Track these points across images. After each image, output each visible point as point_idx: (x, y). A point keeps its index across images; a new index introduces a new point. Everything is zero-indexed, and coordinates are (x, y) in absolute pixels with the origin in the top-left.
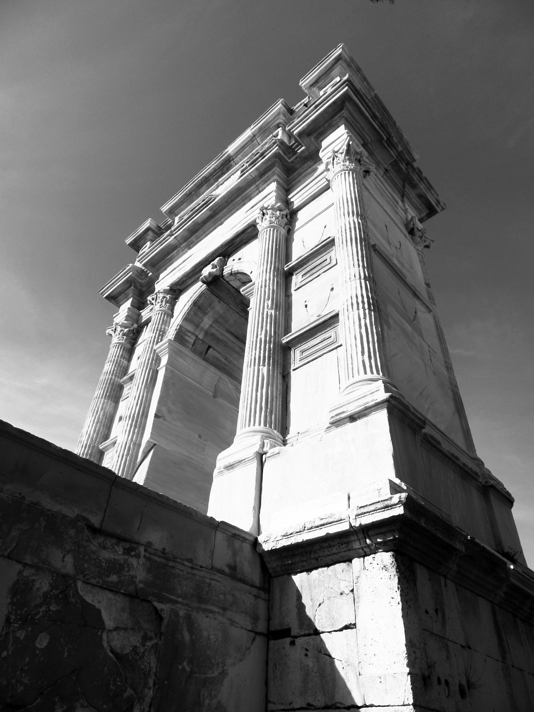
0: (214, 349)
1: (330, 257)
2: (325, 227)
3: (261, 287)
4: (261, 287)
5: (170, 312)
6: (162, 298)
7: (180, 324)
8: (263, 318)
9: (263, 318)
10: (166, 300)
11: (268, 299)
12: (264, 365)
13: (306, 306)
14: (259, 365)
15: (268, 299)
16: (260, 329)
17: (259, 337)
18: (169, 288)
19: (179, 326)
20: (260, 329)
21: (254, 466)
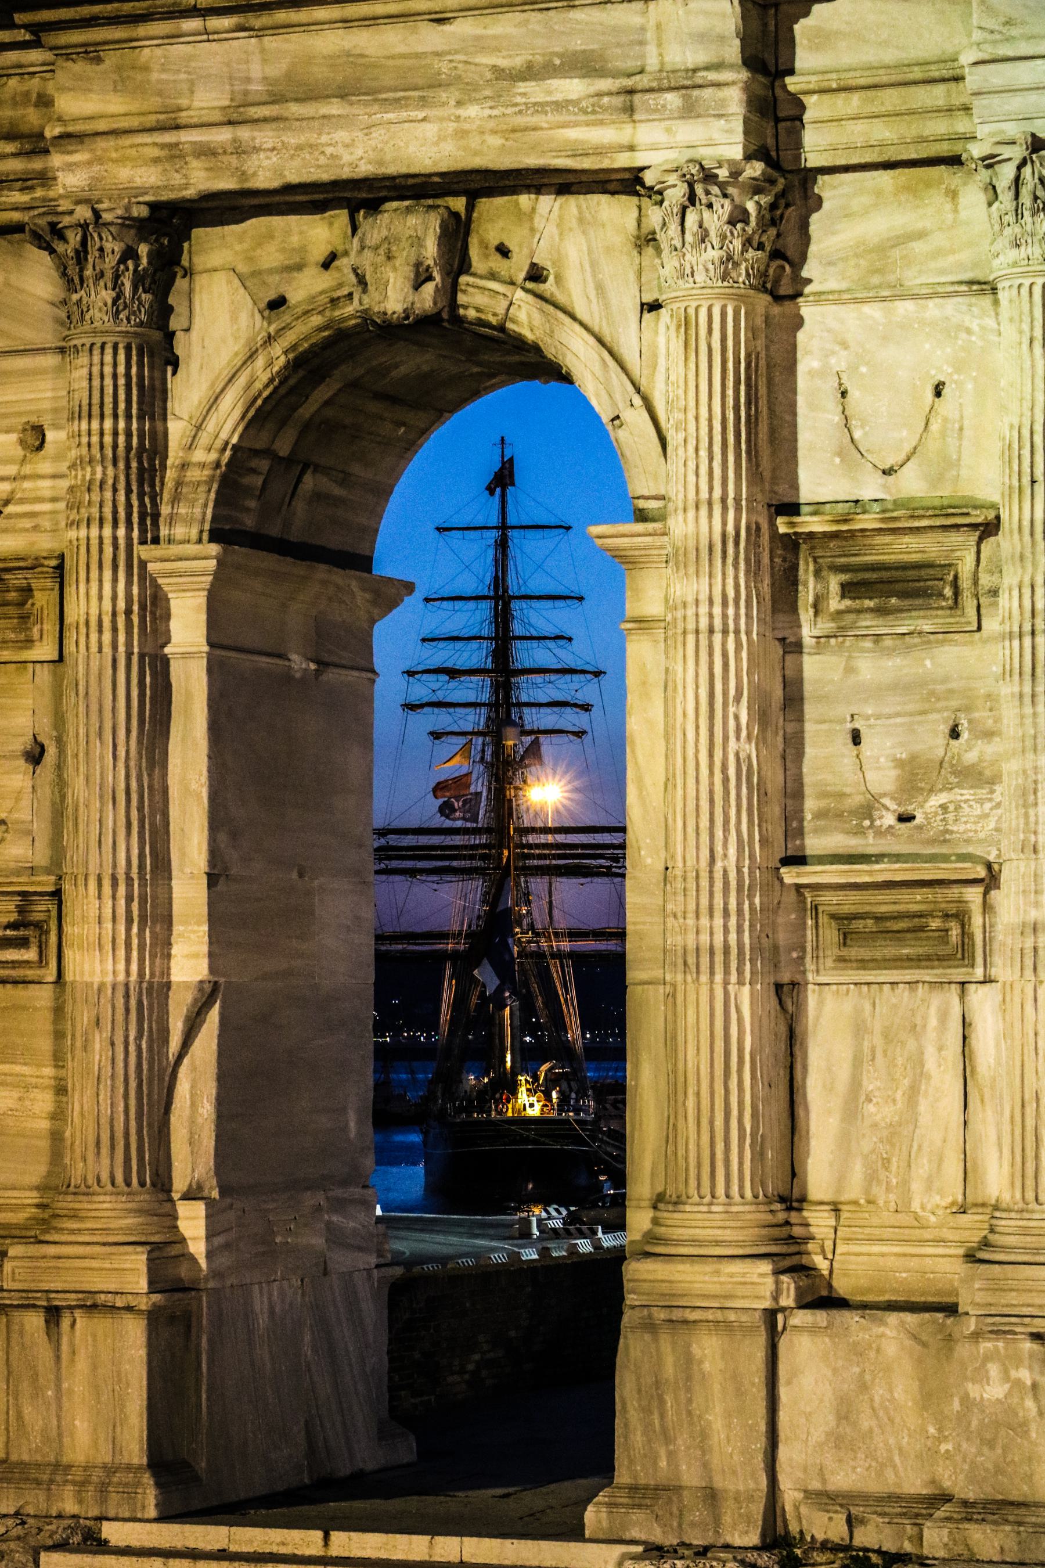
0: (317, 468)
1: (956, 577)
2: (938, 394)
3: (711, 631)
4: (711, 631)
5: (157, 335)
6: (119, 262)
7: (235, 440)
8: (726, 780)
9: (726, 780)
10: (135, 271)
11: (738, 699)
12: (741, 983)
13: (856, 738)
14: (726, 983)
15: (738, 699)
16: (719, 833)
17: (719, 865)
18: (144, 212)
19: (228, 453)
20: (719, 833)
21: (760, 1342)
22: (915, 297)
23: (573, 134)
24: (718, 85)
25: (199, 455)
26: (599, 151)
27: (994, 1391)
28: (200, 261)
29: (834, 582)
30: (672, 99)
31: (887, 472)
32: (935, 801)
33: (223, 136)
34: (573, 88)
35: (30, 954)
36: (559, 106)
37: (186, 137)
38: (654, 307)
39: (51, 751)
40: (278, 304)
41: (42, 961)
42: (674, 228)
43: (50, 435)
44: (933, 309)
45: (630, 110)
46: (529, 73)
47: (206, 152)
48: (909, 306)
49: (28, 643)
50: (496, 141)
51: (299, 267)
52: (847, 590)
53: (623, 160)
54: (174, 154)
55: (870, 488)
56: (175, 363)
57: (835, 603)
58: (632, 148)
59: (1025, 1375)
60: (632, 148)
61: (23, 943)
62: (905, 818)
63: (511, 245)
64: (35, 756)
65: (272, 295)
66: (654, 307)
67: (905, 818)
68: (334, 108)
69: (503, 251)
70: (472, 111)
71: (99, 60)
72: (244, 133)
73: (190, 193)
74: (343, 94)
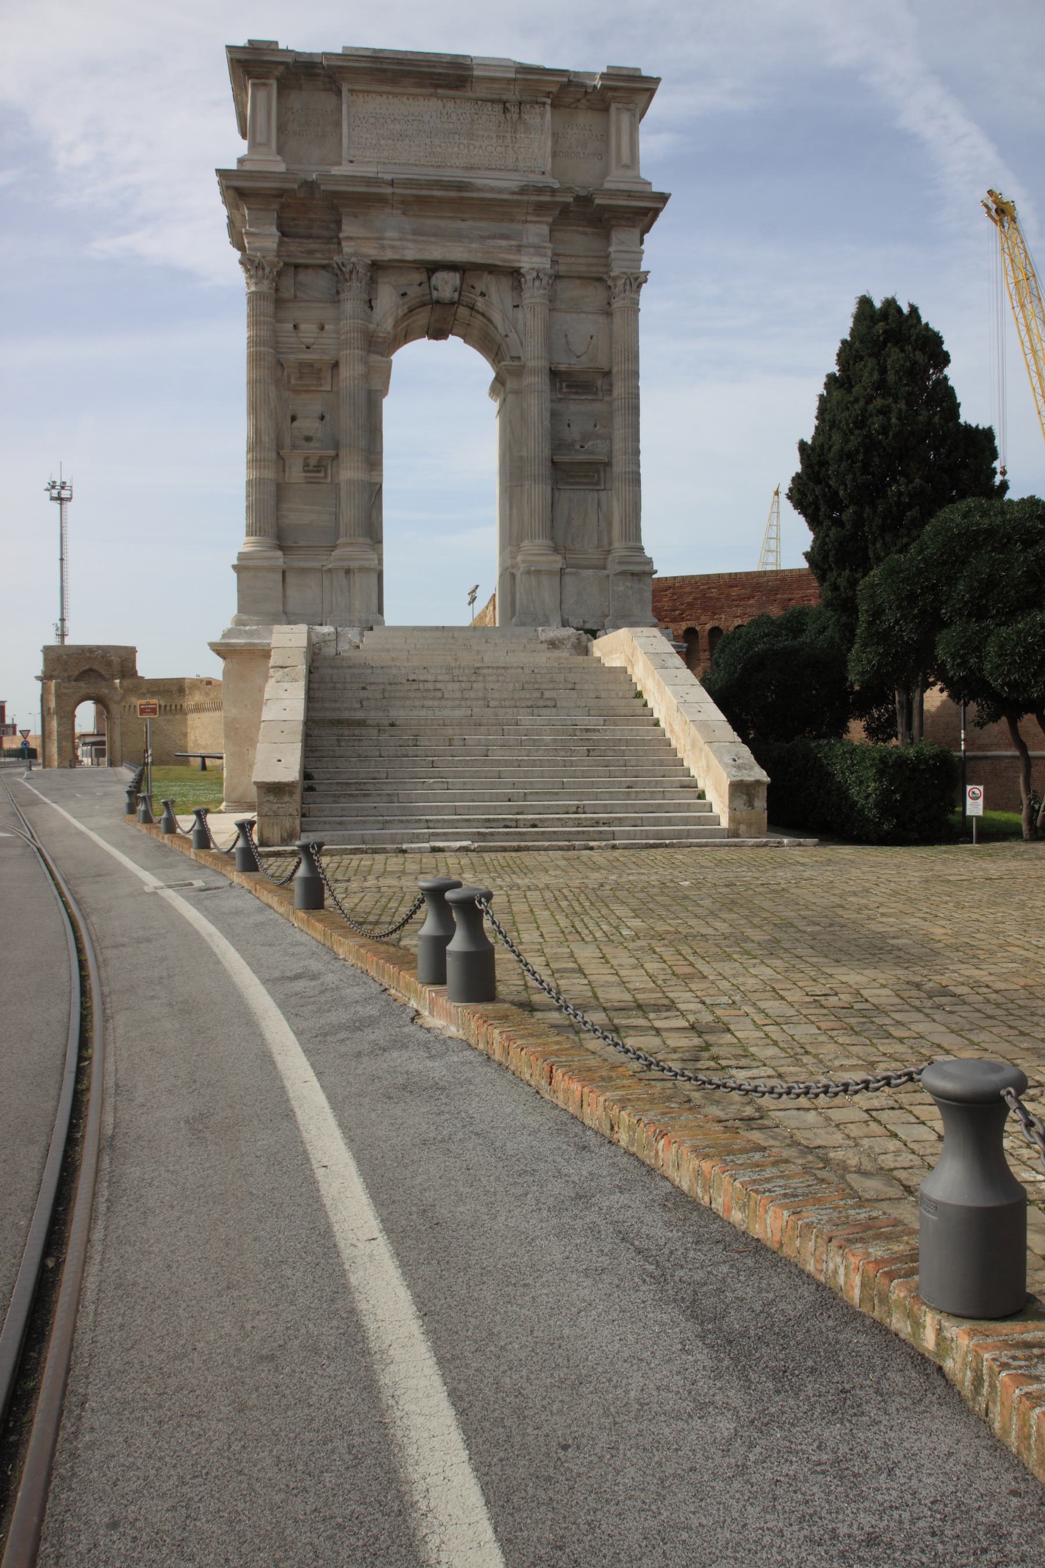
13: (569, 426)
22: (586, 313)
23: (503, 256)
24: (545, 248)
25: (381, 335)
26: (510, 261)
27: (621, 588)
28: (380, 280)
29: (564, 385)
30: (532, 250)
31: (578, 357)
32: (590, 443)
33: (398, 243)
34: (504, 243)
35: (322, 475)
36: (500, 247)
37: (386, 242)
38: (517, 306)
39: (327, 417)
40: (404, 295)
41: (326, 477)
42: (530, 284)
43: (327, 327)
44: (590, 317)
45: (519, 250)
46: (489, 237)
47: (393, 247)
48: (583, 316)
49: (321, 385)
50: (480, 255)
51: (411, 285)
52: (568, 386)
53: (517, 265)
54: (383, 247)
55: (574, 361)
56: (371, 307)
57: (565, 390)
58: (519, 261)
59: (629, 584)
60: (519, 261)
61: (319, 471)
62: (582, 447)
63: (476, 285)
64: (322, 418)
65: (402, 292)
66: (517, 306)
67: (582, 447)
68: (433, 239)
69: (473, 287)
70: (474, 246)
71: (356, 216)
72: (405, 243)
73: (386, 258)
74: (435, 235)
